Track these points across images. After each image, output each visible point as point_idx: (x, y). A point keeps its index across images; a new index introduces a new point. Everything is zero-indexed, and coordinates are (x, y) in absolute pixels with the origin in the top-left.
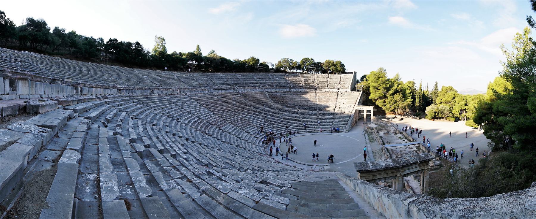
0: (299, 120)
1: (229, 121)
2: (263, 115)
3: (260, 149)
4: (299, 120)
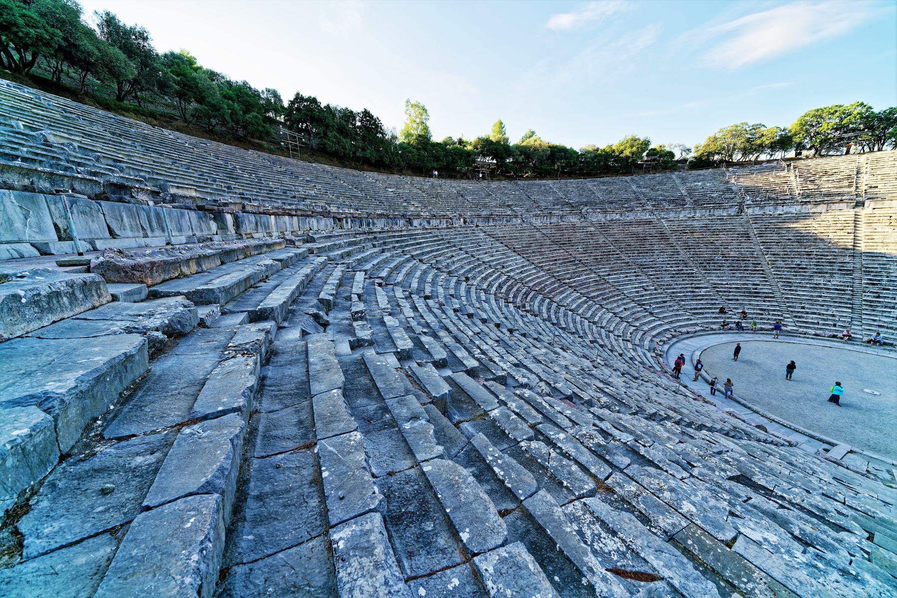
0: (767, 297)
1: (569, 283)
2: (651, 275)
3: (645, 354)
4: (768, 297)
